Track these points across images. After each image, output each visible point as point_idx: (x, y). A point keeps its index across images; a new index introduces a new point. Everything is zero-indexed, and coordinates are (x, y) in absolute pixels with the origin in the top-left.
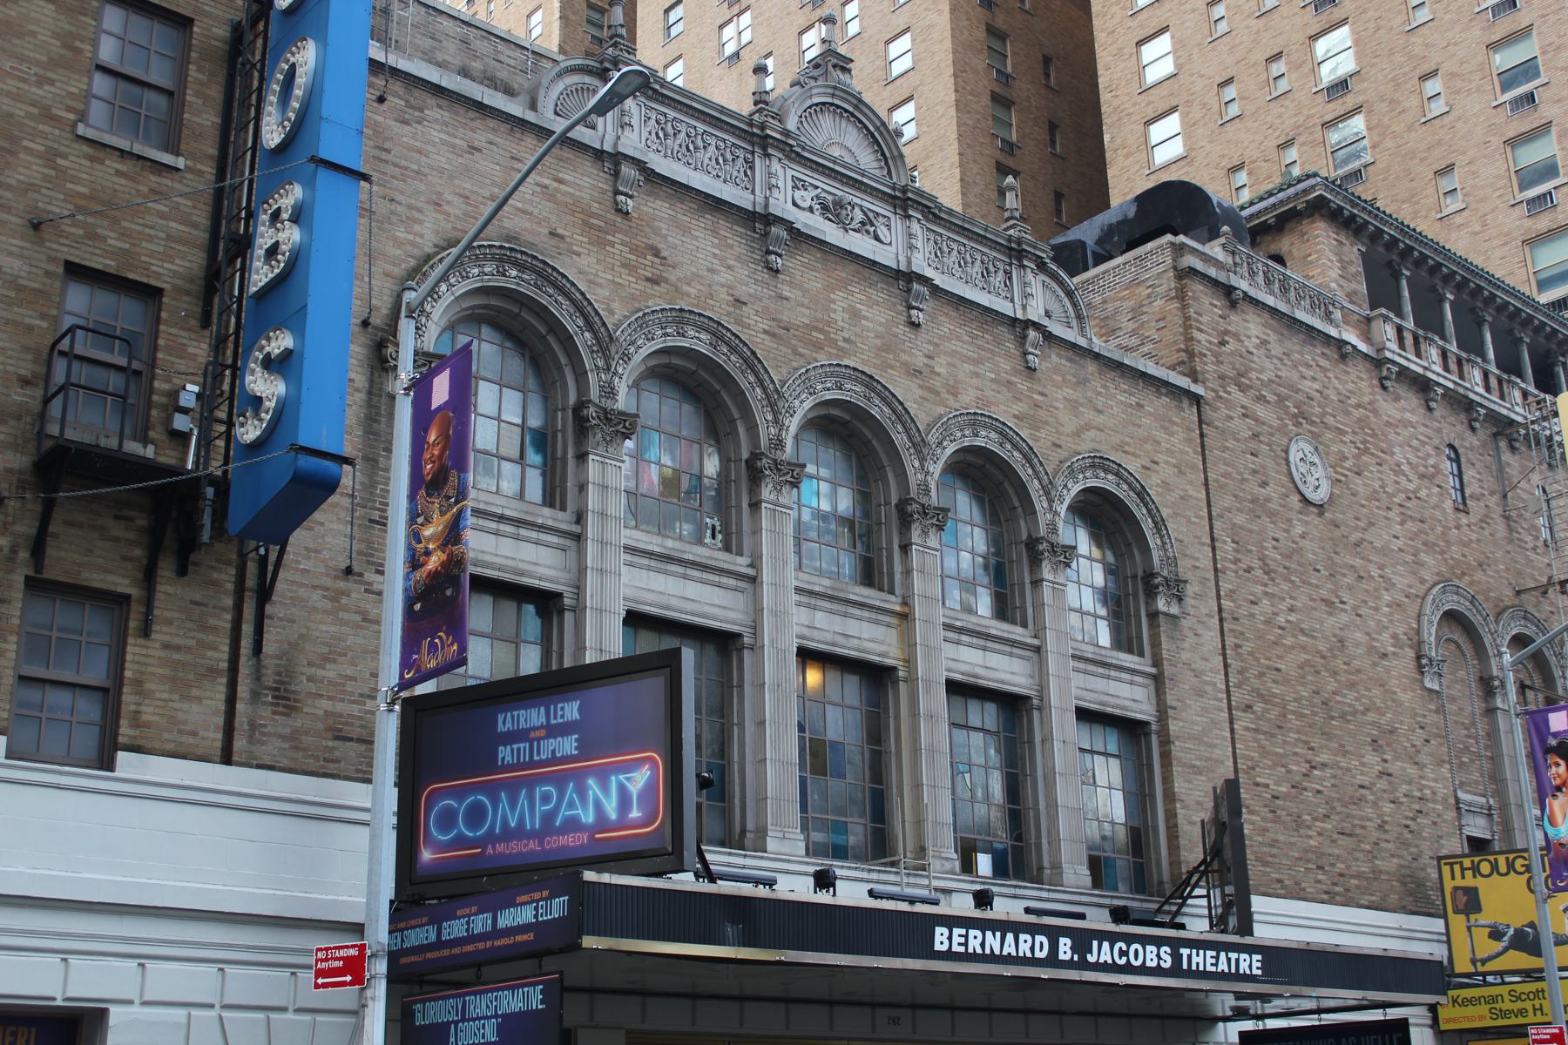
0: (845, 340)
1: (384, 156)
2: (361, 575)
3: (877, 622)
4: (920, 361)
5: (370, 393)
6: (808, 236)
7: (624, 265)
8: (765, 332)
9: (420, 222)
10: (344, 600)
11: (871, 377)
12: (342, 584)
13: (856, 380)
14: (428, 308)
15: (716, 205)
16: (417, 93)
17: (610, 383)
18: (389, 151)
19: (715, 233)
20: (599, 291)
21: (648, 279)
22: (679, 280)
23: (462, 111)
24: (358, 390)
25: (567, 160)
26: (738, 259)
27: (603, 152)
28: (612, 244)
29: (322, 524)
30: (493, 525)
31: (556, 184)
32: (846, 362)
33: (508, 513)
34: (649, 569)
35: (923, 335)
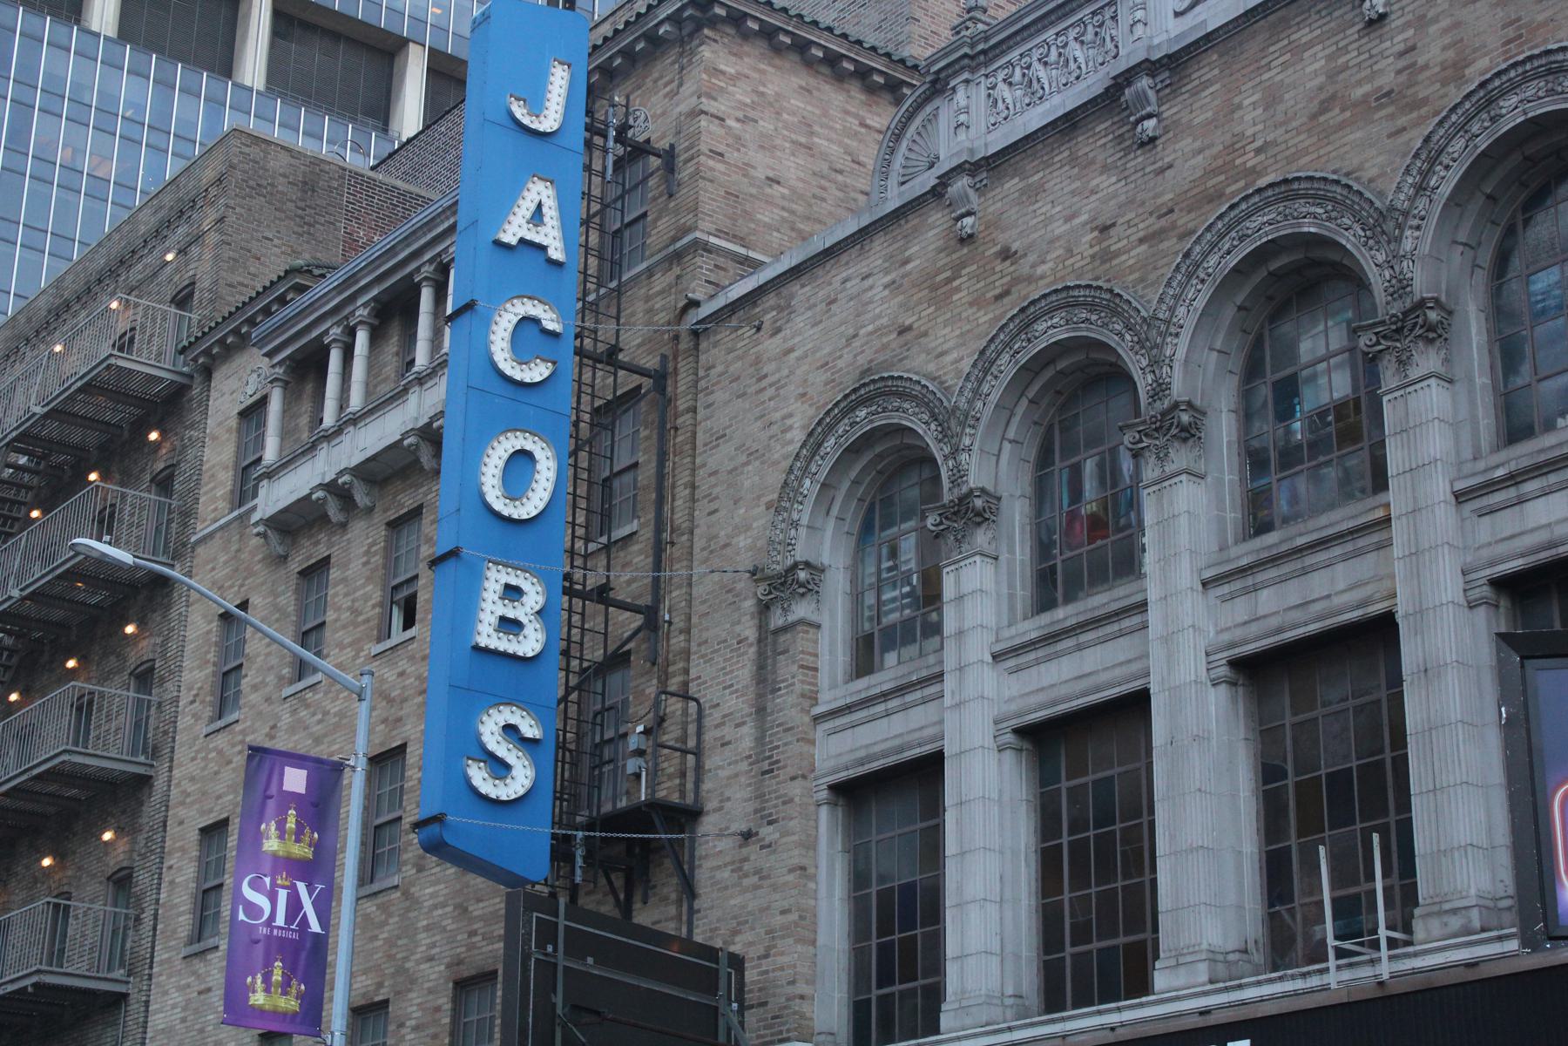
0: (1258, 151)
1: (764, 383)
2: (757, 834)
3: (1358, 554)
4: (1387, 80)
5: (759, 641)
6: (1187, 49)
7: (971, 304)
8: (1141, 241)
9: (791, 428)
10: (746, 867)
11: (1286, 181)
12: (745, 851)
13: (1268, 204)
14: (795, 516)
15: (1068, 125)
16: (784, 291)
17: (958, 466)
18: (765, 376)
19: (1073, 160)
20: (949, 358)
21: (999, 297)
22: (1033, 266)
23: (819, 272)
24: (751, 645)
25: (915, 229)
26: (1105, 169)
27: (934, 188)
28: (958, 289)
29: (729, 799)
30: (880, 708)
31: (902, 271)
32: (1262, 182)
33: (885, 687)
34: (1038, 662)
35: (1395, 22)
